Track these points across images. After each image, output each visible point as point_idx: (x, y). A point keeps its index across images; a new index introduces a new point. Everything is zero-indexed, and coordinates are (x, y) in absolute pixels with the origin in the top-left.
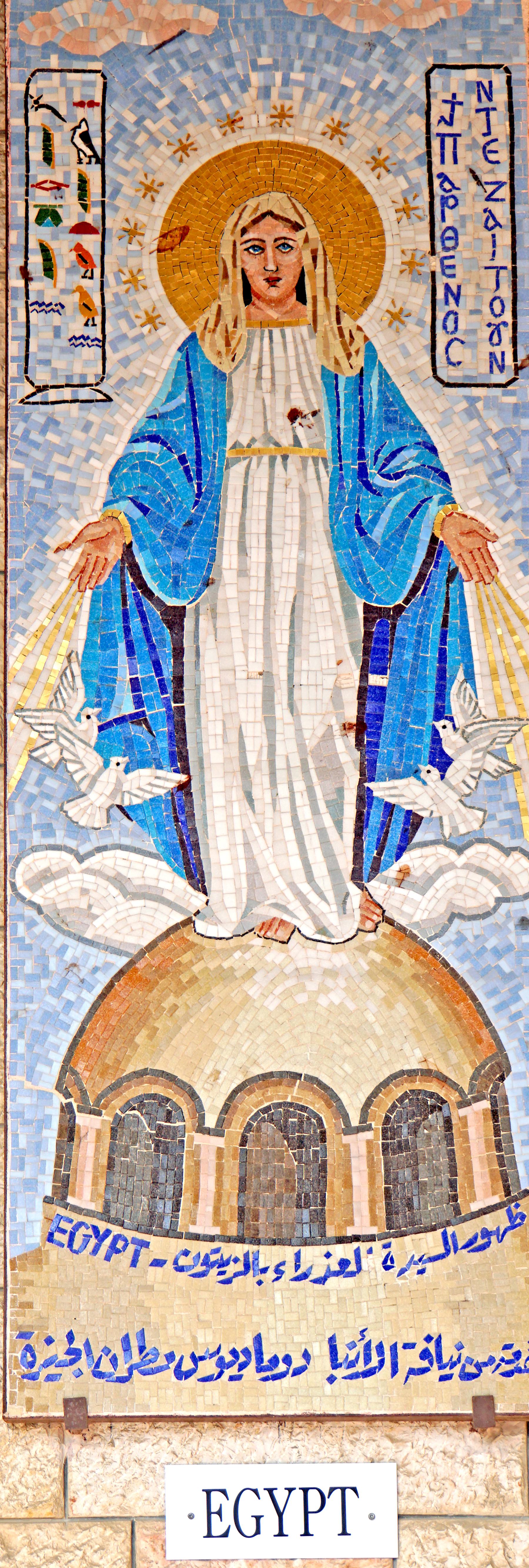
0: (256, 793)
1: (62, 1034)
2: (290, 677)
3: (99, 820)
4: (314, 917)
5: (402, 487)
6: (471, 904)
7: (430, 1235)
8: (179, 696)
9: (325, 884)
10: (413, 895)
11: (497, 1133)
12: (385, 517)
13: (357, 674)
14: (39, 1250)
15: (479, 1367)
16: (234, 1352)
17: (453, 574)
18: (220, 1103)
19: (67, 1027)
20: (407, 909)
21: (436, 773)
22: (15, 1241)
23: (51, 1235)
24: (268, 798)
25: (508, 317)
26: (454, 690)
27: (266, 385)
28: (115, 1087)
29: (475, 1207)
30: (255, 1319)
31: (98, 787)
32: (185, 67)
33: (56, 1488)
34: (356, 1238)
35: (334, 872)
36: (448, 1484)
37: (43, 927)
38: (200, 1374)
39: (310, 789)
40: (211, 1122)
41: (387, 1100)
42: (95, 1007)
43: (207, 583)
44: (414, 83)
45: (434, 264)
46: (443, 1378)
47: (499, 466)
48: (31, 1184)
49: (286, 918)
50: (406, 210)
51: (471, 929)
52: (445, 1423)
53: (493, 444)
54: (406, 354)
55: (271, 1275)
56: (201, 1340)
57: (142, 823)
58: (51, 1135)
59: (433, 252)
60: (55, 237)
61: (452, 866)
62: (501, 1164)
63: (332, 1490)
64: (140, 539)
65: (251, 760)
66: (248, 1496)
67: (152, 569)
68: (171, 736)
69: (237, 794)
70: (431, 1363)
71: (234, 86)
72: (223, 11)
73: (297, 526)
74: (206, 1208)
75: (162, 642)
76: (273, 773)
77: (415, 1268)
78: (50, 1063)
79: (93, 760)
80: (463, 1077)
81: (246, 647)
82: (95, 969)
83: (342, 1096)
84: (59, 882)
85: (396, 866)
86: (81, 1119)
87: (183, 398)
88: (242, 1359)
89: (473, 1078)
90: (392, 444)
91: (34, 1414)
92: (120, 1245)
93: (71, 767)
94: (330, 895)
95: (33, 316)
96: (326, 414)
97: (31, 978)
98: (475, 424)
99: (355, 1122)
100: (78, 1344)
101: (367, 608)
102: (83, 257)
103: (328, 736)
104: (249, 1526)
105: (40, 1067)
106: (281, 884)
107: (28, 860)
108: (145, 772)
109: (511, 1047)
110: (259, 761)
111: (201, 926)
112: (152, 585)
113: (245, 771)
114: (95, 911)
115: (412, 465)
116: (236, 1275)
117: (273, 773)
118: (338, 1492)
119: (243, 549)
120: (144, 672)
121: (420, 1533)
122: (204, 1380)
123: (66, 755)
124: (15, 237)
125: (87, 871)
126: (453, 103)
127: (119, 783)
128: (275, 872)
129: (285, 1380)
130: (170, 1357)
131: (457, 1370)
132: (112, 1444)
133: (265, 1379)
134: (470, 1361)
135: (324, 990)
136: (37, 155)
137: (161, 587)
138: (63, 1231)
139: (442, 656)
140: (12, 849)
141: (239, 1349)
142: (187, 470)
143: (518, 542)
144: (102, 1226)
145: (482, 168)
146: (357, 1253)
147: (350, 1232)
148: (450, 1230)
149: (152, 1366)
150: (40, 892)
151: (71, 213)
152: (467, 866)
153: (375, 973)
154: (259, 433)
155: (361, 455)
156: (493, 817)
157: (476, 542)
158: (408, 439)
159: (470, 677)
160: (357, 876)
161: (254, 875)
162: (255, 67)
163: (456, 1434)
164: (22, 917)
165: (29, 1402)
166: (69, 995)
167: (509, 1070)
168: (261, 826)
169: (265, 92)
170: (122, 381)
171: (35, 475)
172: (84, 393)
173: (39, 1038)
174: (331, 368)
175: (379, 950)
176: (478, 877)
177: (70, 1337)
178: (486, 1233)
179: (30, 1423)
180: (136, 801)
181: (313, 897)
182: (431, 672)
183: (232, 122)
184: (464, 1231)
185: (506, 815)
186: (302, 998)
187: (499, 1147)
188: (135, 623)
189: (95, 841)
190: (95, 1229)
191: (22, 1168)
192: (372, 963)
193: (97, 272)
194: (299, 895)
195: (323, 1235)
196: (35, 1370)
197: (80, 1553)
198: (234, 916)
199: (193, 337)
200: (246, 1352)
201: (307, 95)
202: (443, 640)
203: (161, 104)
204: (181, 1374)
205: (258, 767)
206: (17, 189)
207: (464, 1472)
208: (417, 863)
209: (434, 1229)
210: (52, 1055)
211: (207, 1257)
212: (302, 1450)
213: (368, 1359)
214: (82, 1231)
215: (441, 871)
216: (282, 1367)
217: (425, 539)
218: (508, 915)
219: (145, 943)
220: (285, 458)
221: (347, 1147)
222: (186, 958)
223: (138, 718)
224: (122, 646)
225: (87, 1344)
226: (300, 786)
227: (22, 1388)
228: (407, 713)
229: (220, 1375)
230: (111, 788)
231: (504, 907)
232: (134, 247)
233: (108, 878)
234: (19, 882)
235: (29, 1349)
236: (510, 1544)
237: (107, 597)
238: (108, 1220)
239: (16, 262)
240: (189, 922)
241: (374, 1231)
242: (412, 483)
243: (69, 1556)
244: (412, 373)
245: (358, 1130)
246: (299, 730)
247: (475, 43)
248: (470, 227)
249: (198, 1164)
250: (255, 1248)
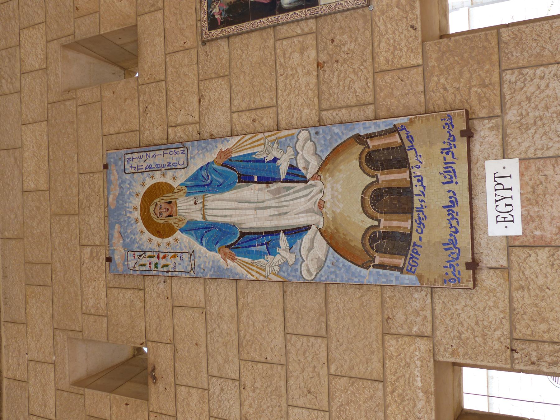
0: (285, 211)
1: (352, 268)
2: (256, 203)
3: (293, 256)
4: (317, 194)
5: (211, 175)
6: (312, 149)
7: (409, 154)
8: (261, 233)
9: (308, 191)
10: (310, 165)
11: (377, 136)
12: (218, 179)
13: (254, 184)
14: (417, 276)
15: (450, 136)
16: (449, 215)
17: (230, 160)
18: (370, 220)
19: (350, 266)
20: (314, 167)
21: (278, 161)
22: (415, 284)
23: (412, 272)
24: (286, 208)
25: (173, 150)
26: (257, 158)
27: (189, 211)
28: (367, 252)
29: (399, 141)
30: (437, 208)
31: (285, 256)
32: (126, 232)
33: (498, 272)
34: (410, 177)
35: (305, 188)
36: (492, 144)
37: (322, 272)
38: (456, 226)
39: (284, 196)
40: (376, 223)
41: (368, 170)
42: (344, 258)
43: (234, 226)
44: (128, 177)
45: (163, 169)
46: (455, 147)
47: (205, 150)
48: (397, 278)
49: (318, 202)
50: (152, 177)
51: (319, 148)
52: (471, 146)
53: (200, 152)
54: (182, 175)
55: (423, 203)
56: (445, 225)
57: (294, 243)
58: (382, 271)
59: (161, 170)
60: (160, 264)
61: (302, 155)
62: (386, 134)
63: (495, 181)
64: (224, 244)
65: (276, 213)
66: (498, 209)
67: (231, 241)
68: (271, 235)
69: (285, 217)
70: (450, 151)
71: (130, 220)
72: (116, 223)
73: (220, 202)
74: (403, 224)
75: (248, 237)
76: (280, 207)
77: (419, 158)
78: (360, 271)
79: (278, 257)
80: (359, 148)
81: (249, 215)
82: (333, 257)
83: (367, 184)
84: (310, 267)
85: (303, 171)
86: (377, 262)
87: (193, 232)
88: (451, 212)
89: (361, 144)
90: (201, 178)
91: (472, 279)
92: (415, 251)
93: (280, 263)
94: (311, 189)
95: (177, 270)
96: (195, 195)
97: (337, 276)
98: (196, 157)
99: (375, 179)
100: (448, 264)
101: (239, 182)
102: (164, 257)
103: (269, 192)
104: (509, 208)
105: (362, 274)
106: (309, 203)
107: (304, 276)
108: (281, 242)
109: (351, 134)
110: (277, 211)
111: (321, 227)
112: (235, 240)
113: (280, 215)
114: (317, 257)
115: (205, 173)
116: (423, 214)
117: (280, 207)
118: (496, 179)
119: (226, 216)
120: (256, 242)
121: (509, 151)
122: (458, 224)
123: (277, 264)
124: (161, 274)
125: (307, 259)
126: (131, 167)
127: (283, 250)
128: (306, 205)
129: (457, 198)
130: (451, 235)
131: (452, 143)
132: (482, 253)
133: (457, 204)
134: (449, 139)
135: (337, 190)
136: (144, 268)
137: (235, 238)
138: (411, 268)
139: (250, 161)
140: (302, 281)
141: (448, 213)
142: (209, 231)
143: (222, 143)
144: (409, 256)
145: (144, 159)
146: (415, 177)
147: (408, 179)
148: (407, 148)
149: (454, 241)
150: (313, 273)
151: (155, 260)
152: (302, 151)
153: (332, 176)
154: (199, 212)
155: (204, 186)
156: (289, 144)
157: (223, 154)
158: (200, 174)
159: (254, 153)
160: (306, 182)
161: (308, 211)
162: (126, 215)
163: (475, 142)
164: (320, 279)
165: (468, 281)
166: (341, 265)
167: (358, 134)
168: (293, 210)
169: (131, 212)
170: (190, 248)
171: (211, 271)
172: (192, 258)
173: (353, 274)
174: (185, 194)
175: (326, 175)
176: (305, 147)
177: (445, 267)
178: (407, 137)
179: (475, 280)
180: (288, 245)
181: (312, 194)
182: (253, 164)
183: (137, 220)
184: (407, 144)
185: (288, 140)
186: (340, 196)
187: (381, 135)
188: (243, 245)
189: (299, 257)
190: (410, 258)
191: (392, 281)
192: (329, 176)
193: (167, 254)
194: (311, 198)
195: (410, 188)
196: (456, 278)
197: (521, 264)
198: (318, 217)
199: (180, 230)
200: (448, 211)
201: (131, 202)
202: (245, 161)
203: (134, 238)
204: (457, 232)
205: (278, 211)
206: (151, 273)
207: (487, 139)
208: (302, 165)
209: (407, 153)
210: (358, 270)
211: (418, 224)
212: (481, 192)
213: (450, 172)
214: (411, 262)
215: (304, 158)
216: (453, 199)
217: (222, 168)
218: (315, 138)
219: (326, 243)
220: (205, 206)
221: (383, 181)
222: (329, 230)
223: (267, 244)
224: (250, 249)
225: (448, 262)
226: (283, 199)
227: (463, 283)
228: (263, 170)
229: (457, 219)
230: (285, 252)
231: (313, 139)
232: (162, 244)
233: (309, 253)
234: (310, 279)
235: (450, 280)
236: (512, 122)
237: (238, 252)
238: (407, 254)
239: (165, 274)
240: (320, 230)
241: (408, 172)
242: (209, 172)
243: (522, 268)
244: (186, 173)
245: (377, 178)
246: (269, 200)
247: (120, 163)
248: (155, 161)
249: (389, 227)
250: (415, 209)
